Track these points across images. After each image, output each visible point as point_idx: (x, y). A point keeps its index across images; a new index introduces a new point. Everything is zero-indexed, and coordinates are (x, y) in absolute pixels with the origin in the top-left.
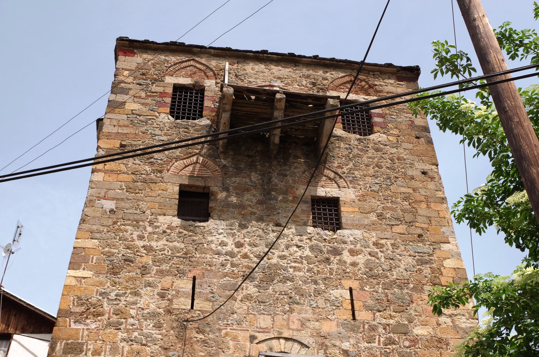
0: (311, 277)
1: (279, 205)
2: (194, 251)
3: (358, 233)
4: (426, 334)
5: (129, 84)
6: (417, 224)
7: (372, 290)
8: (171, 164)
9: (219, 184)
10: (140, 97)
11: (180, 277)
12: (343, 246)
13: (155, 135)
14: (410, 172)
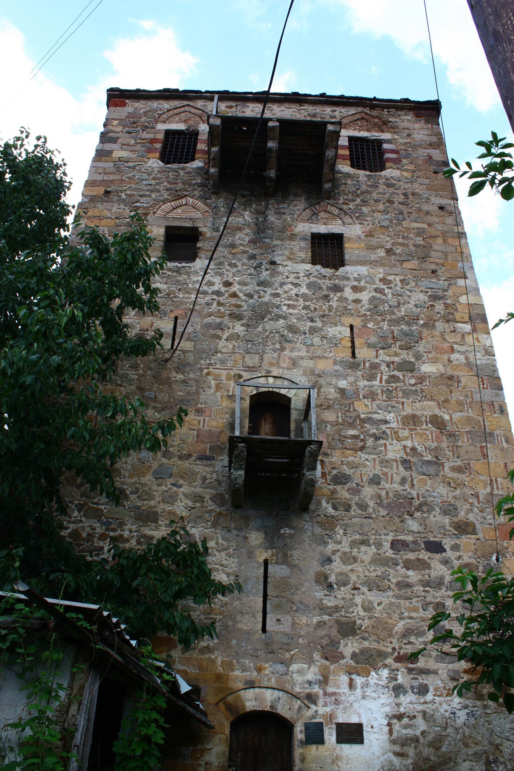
0: (307, 314)
1: (275, 242)
2: (177, 291)
3: (363, 270)
4: (435, 371)
5: (118, 133)
6: (431, 260)
7: (376, 327)
8: (157, 207)
9: (209, 225)
10: (128, 145)
11: (161, 317)
12: (345, 283)
13: (143, 180)
14: (425, 208)
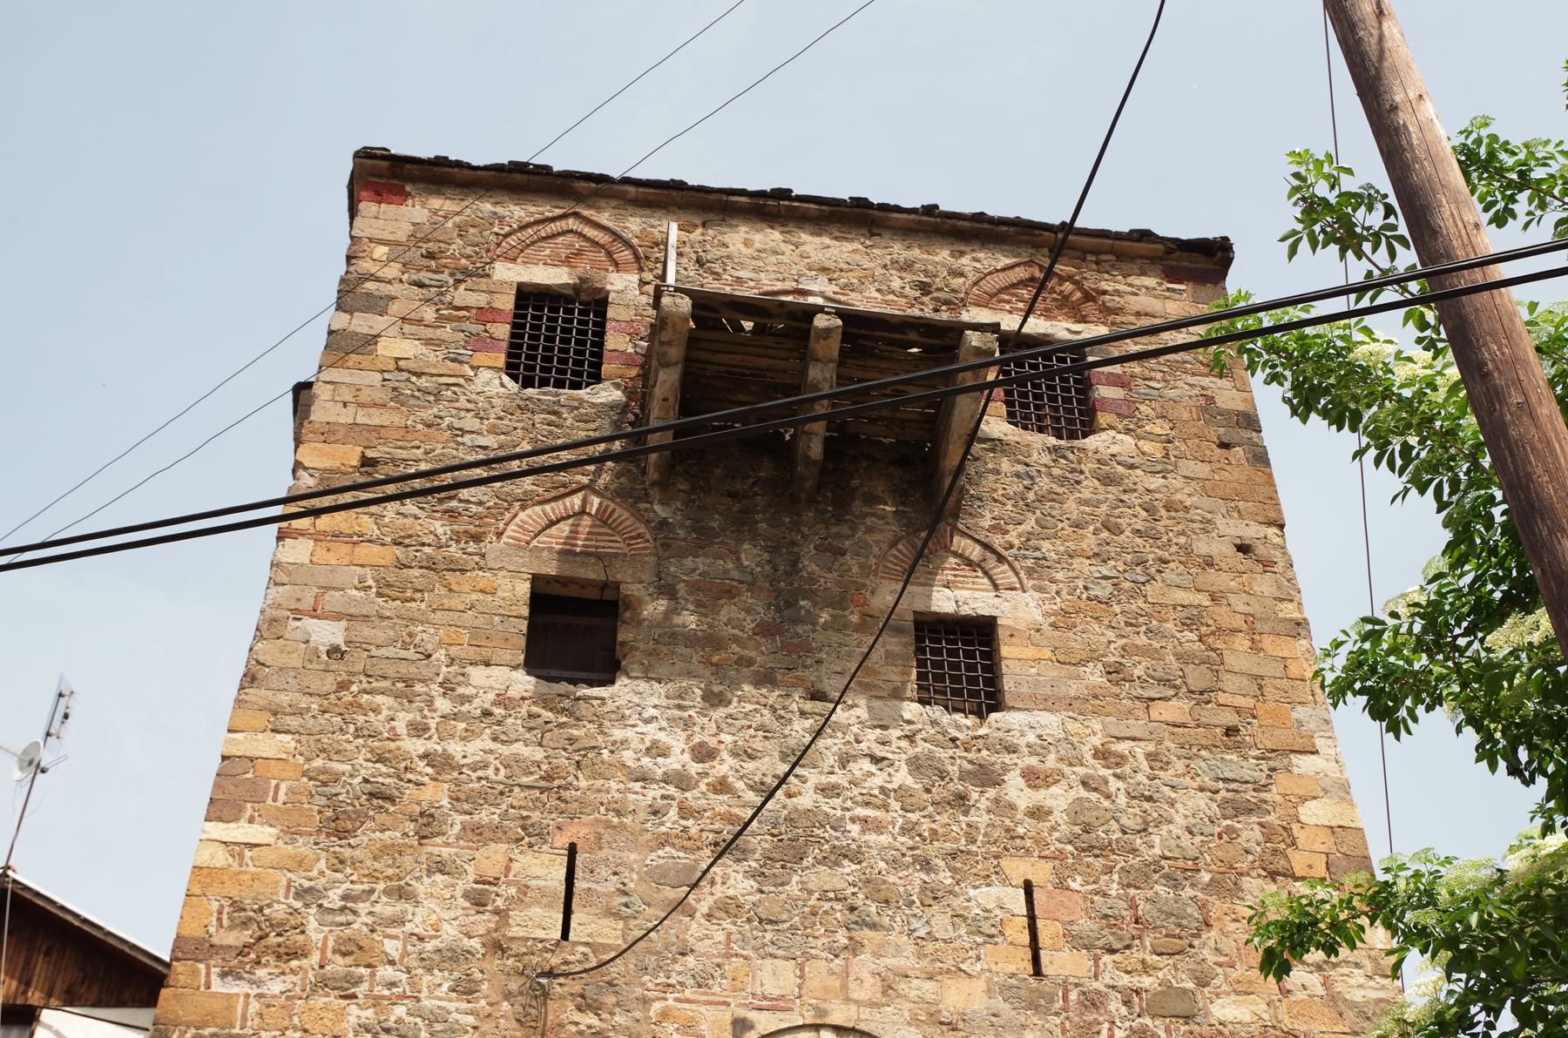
0: (912, 849)
1: (820, 637)
2: (572, 769)
3: (1050, 723)
4: (1247, 1018)
5: (389, 282)
7: (1090, 887)
8: (508, 516)
9: (648, 576)
10: (420, 322)
11: (531, 846)
12: (1008, 759)
13: (464, 432)
14: (1202, 547)
